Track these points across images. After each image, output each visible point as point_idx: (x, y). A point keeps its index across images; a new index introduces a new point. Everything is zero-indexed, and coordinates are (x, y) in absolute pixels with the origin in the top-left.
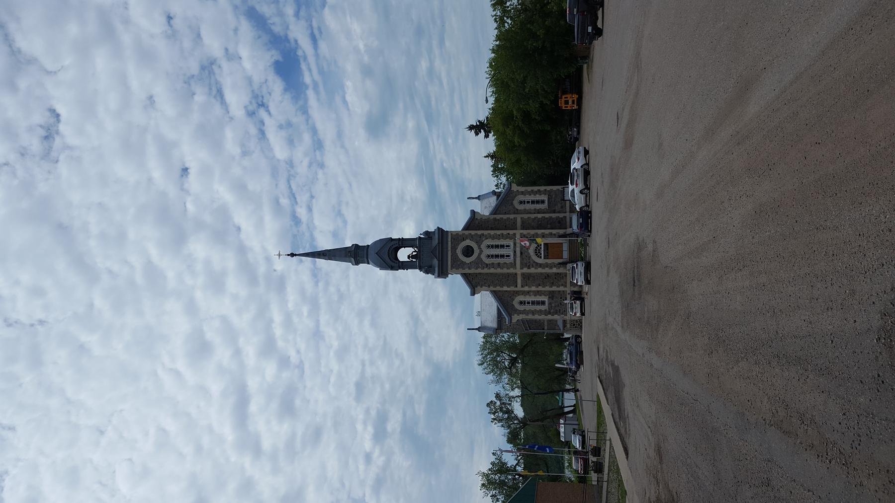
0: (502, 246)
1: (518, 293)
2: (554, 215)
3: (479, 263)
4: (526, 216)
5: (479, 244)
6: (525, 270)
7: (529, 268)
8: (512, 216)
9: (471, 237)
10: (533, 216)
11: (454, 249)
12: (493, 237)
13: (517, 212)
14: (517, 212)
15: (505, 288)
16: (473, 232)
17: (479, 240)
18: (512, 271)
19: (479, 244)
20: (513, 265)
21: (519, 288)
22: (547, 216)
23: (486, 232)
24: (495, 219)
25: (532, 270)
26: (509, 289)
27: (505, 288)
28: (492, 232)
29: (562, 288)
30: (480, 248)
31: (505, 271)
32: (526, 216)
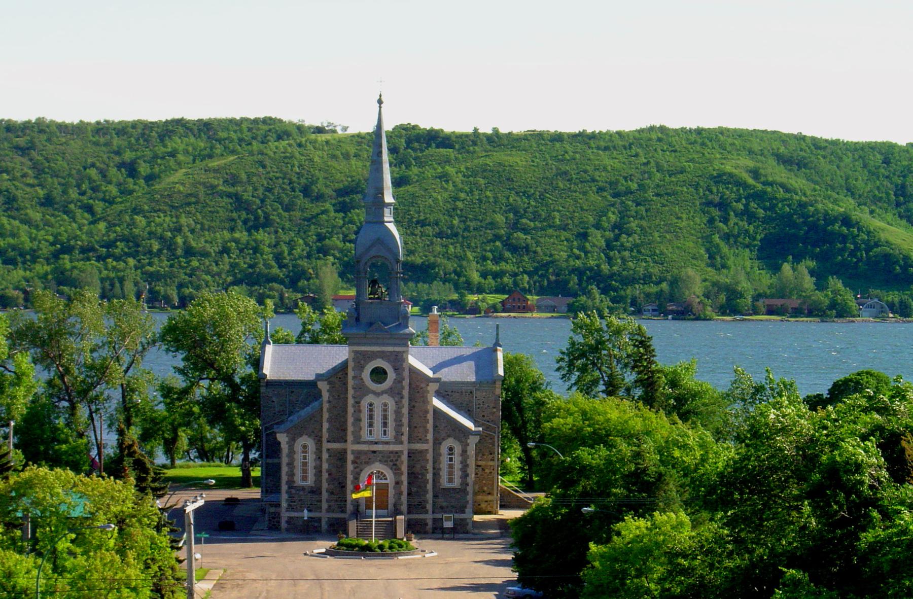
0: (385, 424)
1: (319, 441)
2: (430, 496)
3: (362, 391)
4: (430, 456)
5: (391, 392)
6: (350, 457)
7: (354, 462)
8: (430, 436)
9: (399, 381)
10: (430, 467)
11: (382, 355)
12: (398, 412)
13: (437, 443)
14: (437, 443)
15: (326, 425)
16: (406, 383)
17: (395, 392)
18: (350, 438)
19: (391, 392)
20: (358, 441)
21: (326, 445)
22: (430, 486)
23: (406, 402)
24: (427, 412)
25: (350, 467)
26: (324, 430)
27: (326, 425)
28: (405, 411)
29: (325, 505)
30: (383, 393)
31: (350, 429)
32: (430, 456)
